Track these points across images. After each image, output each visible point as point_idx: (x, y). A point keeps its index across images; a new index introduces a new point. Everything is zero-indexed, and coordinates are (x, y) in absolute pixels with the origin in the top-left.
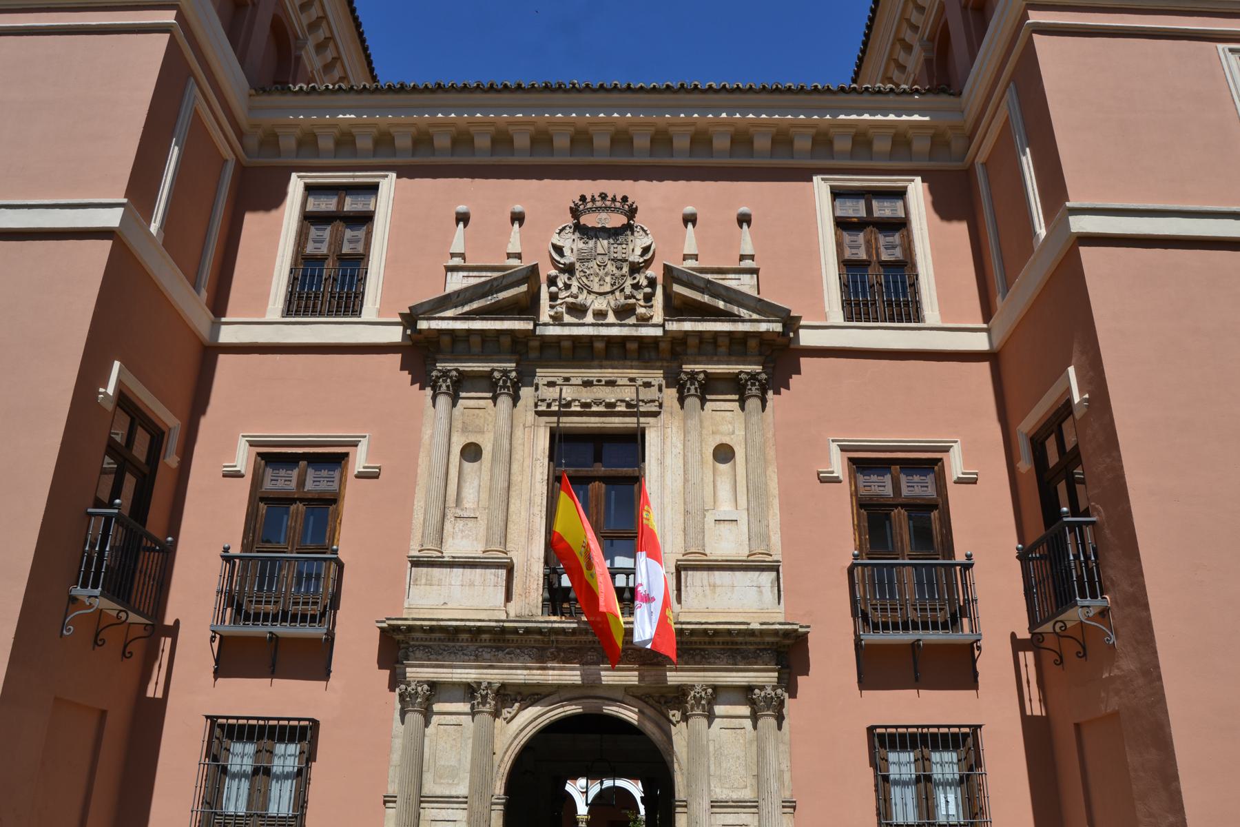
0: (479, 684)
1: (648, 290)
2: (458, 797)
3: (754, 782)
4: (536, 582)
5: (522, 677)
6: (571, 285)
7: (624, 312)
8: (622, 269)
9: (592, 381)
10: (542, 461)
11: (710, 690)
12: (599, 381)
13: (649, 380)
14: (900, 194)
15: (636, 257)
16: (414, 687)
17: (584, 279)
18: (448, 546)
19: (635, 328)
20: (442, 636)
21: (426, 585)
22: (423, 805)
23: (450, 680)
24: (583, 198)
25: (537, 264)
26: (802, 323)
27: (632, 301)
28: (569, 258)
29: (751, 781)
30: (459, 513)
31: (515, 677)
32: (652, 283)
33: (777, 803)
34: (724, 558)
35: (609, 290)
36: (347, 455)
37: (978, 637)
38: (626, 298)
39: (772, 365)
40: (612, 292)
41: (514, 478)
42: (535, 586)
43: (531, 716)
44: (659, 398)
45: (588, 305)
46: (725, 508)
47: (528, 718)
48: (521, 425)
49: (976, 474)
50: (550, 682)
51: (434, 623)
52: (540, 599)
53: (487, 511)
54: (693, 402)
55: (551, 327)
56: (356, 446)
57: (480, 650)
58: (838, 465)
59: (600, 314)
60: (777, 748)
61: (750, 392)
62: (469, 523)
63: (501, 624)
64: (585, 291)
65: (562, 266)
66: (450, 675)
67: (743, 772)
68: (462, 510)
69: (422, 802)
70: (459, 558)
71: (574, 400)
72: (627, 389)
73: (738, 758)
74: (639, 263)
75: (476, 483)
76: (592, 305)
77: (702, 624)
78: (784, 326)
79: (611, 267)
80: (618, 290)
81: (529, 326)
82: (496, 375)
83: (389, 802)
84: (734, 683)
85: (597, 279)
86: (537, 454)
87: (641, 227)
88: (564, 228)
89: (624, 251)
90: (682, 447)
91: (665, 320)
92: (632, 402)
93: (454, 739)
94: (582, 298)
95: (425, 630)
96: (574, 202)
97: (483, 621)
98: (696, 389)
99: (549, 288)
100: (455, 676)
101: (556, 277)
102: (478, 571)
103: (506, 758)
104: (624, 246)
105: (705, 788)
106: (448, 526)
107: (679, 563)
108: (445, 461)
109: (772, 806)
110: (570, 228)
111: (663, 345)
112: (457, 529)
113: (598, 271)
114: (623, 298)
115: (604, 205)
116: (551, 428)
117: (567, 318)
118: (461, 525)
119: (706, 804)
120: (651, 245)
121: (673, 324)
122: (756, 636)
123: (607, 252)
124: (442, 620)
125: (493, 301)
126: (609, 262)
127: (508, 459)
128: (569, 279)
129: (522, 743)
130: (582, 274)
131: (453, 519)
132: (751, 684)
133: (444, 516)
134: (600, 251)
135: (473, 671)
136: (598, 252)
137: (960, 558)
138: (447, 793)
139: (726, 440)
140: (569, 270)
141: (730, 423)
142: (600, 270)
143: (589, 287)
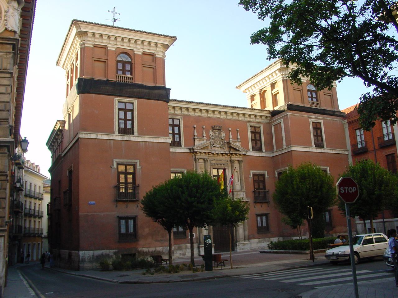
14: (259, 127)
27: (223, 146)
38: (221, 145)
58: (251, 176)
82: (205, 159)
111: (228, 155)
117: (213, 148)
139: (237, 171)
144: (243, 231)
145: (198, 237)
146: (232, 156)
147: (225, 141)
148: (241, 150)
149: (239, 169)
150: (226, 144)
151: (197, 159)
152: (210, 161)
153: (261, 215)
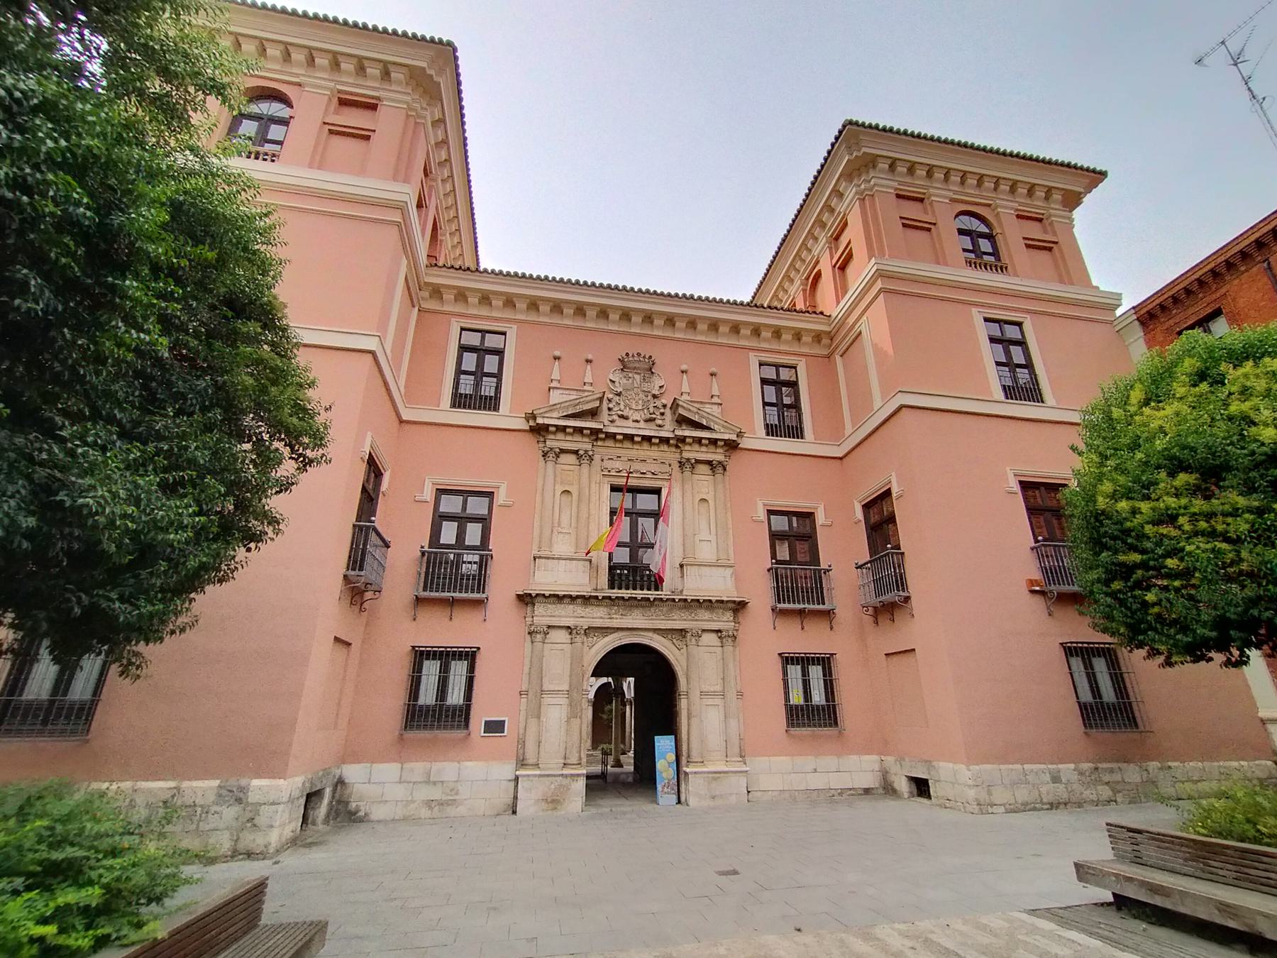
3: (721, 681)
30: (560, 530)
33: (735, 693)
54: (687, 474)
72: (652, 465)
109: (732, 695)
111: (671, 442)
135: (572, 619)
146: (687, 448)
153: (804, 661)
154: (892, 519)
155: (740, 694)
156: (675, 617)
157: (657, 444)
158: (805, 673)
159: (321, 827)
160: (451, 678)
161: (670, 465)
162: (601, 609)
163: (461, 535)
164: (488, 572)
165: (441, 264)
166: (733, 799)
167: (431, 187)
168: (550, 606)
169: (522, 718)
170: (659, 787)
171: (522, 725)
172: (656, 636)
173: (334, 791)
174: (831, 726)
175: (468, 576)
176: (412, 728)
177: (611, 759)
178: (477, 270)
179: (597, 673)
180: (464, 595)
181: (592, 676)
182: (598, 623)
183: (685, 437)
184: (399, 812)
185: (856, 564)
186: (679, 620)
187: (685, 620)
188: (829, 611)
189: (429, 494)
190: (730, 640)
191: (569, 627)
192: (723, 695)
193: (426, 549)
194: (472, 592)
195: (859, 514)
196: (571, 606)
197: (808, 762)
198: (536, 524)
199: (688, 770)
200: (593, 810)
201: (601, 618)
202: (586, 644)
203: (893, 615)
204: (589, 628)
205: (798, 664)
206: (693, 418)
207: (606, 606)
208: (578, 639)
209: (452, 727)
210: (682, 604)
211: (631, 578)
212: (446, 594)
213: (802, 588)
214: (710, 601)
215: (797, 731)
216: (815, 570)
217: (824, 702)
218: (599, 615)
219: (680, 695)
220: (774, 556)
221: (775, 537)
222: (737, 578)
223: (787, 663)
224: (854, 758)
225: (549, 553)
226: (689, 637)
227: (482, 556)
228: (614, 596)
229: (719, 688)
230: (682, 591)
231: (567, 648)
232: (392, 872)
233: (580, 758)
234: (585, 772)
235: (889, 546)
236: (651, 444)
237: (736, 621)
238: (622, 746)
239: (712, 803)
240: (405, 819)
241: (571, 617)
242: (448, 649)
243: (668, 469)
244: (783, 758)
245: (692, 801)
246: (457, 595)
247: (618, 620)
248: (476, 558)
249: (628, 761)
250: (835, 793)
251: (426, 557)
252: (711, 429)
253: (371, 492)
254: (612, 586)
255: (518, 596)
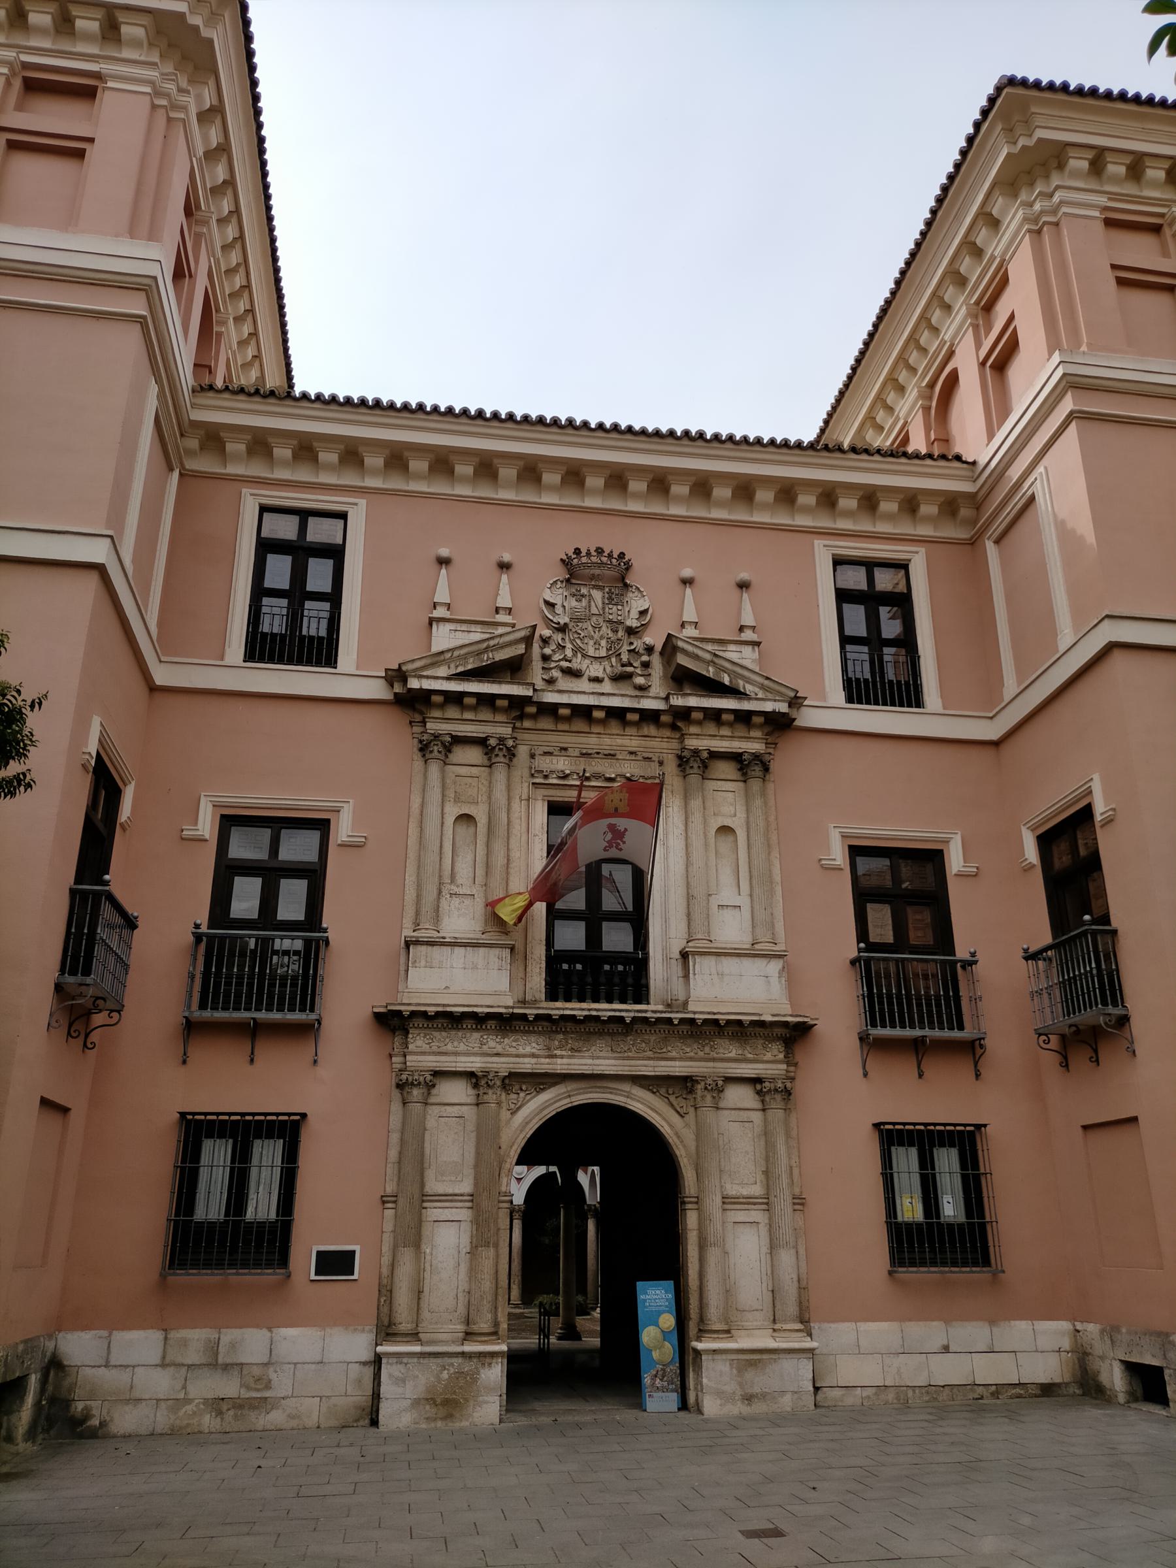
0: (486, 1073)
1: (645, 658)
2: (462, 1195)
4: (538, 966)
5: (529, 1066)
6: (564, 647)
7: (620, 678)
8: (617, 632)
9: (591, 754)
10: (541, 836)
11: (720, 1083)
12: (598, 753)
13: (650, 755)
15: (632, 622)
16: (416, 1077)
17: (578, 641)
18: (443, 925)
19: (637, 699)
20: (445, 1021)
21: (426, 967)
22: (425, 1205)
23: (454, 1069)
24: (577, 551)
25: (536, 625)
26: (806, 703)
27: (629, 669)
28: (564, 620)
29: (760, 1177)
30: (455, 889)
31: (523, 1066)
32: (650, 650)
33: (789, 1200)
34: (728, 946)
35: (605, 655)
36: (328, 821)
37: (982, 1036)
38: (623, 665)
39: (773, 746)
40: (608, 657)
41: (512, 854)
42: (538, 971)
43: (537, 1107)
44: (659, 774)
45: (584, 669)
46: (727, 894)
47: (535, 1109)
48: (518, 797)
49: (977, 868)
50: (559, 1072)
51: (440, 1009)
52: (544, 983)
53: (484, 888)
54: (694, 779)
55: (550, 694)
56: (339, 811)
57: (485, 1037)
58: (839, 855)
59: (597, 680)
60: (787, 1142)
61: (753, 773)
62: (465, 901)
63: (511, 1010)
64: (579, 655)
65: (556, 626)
66: (454, 1064)
67: (753, 1168)
68: (458, 886)
69: (423, 1201)
70: (461, 939)
71: (572, 773)
73: (747, 1153)
74: (637, 628)
75: (470, 857)
76: (588, 671)
77: (714, 1014)
78: (790, 706)
79: (606, 630)
80: (614, 655)
81: (530, 693)
82: (493, 742)
83: (388, 1202)
84: (744, 1075)
85: (591, 643)
86: (535, 829)
87: (637, 587)
88: (555, 582)
89: (619, 613)
90: (684, 828)
91: (669, 694)
92: (633, 778)
93: (456, 1133)
94: (576, 664)
95: (430, 1016)
96: (567, 555)
97: (492, 1007)
98: (699, 767)
99: (542, 648)
100: (458, 1065)
101: (550, 637)
102: (482, 950)
103: (512, 1153)
104: (620, 607)
105: (718, 1184)
106: (444, 903)
107: (687, 949)
108: (439, 834)
109: (783, 1204)
110: (562, 582)
111: (664, 718)
112: (453, 907)
113: (593, 633)
114: (619, 665)
115: (599, 562)
116: (548, 801)
117: (564, 683)
118: (458, 902)
119: (718, 1200)
120: (648, 609)
121: (678, 698)
122: (767, 1028)
123: (601, 613)
124: (448, 1005)
125: (489, 662)
126: (604, 625)
127: (506, 835)
128: (563, 639)
129: (528, 1136)
130: (576, 636)
131: (448, 896)
132: (760, 1076)
133: (440, 892)
134: (594, 610)
135: (478, 1059)
136: (592, 612)
137: (962, 953)
138: (450, 1191)
139: (728, 822)
140: (562, 629)
141: (732, 805)
142: (595, 632)
143: (584, 650)
144: (765, 1250)
145: (385, 1271)
146: (693, 729)
147: (648, 640)
148: (749, 688)
149: (741, 815)
150: (656, 660)
151: (436, 737)
152: (532, 756)
154: (1093, 863)
155: (799, 1202)
156: (674, 1054)
157: (637, 724)
158: (926, 1163)
159: (23, 1446)
160: (254, 1172)
161: (661, 763)
162: (533, 1038)
163: (269, 901)
164: (320, 972)
165: (219, 383)
166: (786, 1402)
167: (198, 237)
168: (436, 1034)
169: (386, 1248)
170: (647, 1380)
171: (386, 1260)
172: (638, 1092)
173: (44, 1382)
174: (975, 1264)
175: (284, 978)
176: (183, 1265)
177: (556, 1324)
178: (289, 395)
179: (527, 1157)
180: (276, 1016)
181: (518, 1163)
182: (527, 1065)
183: (689, 710)
184: (163, 1420)
185: (1026, 951)
186: (681, 1059)
187: (691, 1059)
188: (973, 1042)
189: (206, 825)
190: (778, 1097)
191: (470, 1075)
192: (766, 1203)
193: (204, 929)
194: (292, 1009)
195: (1031, 853)
196: (476, 1035)
197: (932, 1333)
198: (410, 879)
199: (700, 1346)
200: (521, 1421)
201: (533, 1056)
202: (504, 1105)
203: (1096, 1051)
204: (512, 1075)
205: (911, 1144)
206: (704, 673)
207: (539, 1033)
208: (491, 1096)
209: (257, 1265)
210: (685, 1028)
211: (589, 980)
212: (244, 1015)
213: (919, 999)
214: (739, 1022)
215: (909, 1274)
216: (942, 962)
217: (962, 1218)
218: (528, 1050)
219: (684, 1203)
220: (862, 933)
221: (863, 896)
222: (790, 976)
223: (891, 1143)
224: (1023, 1325)
225: (435, 934)
226: (699, 1093)
227: (308, 942)
228: (556, 1013)
229: (757, 1190)
230: (686, 1003)
231: (469, 1112)
232: (158, 1525)
233: (496, 1324)
234: (504, 1348)
235: (1087, 917)
236: (625, 723)
237: (790, 1060)
238: (580, 1298)
239: (745, 1410)
240: (173, 1433)
241: (475, 1054)
242: (248, 1118)
243: (653, 770)
244: (884, 1325)
245: (711, 1406)
246: (262, 1015)
247: (565, 1061)
248: (298, 945)
249: (591, 1327)
250: (985, 1394)
251: (203, 946)
252: (739, 693)
253: (101, 826)
254: (552, 996)
255: (377, 1016)
